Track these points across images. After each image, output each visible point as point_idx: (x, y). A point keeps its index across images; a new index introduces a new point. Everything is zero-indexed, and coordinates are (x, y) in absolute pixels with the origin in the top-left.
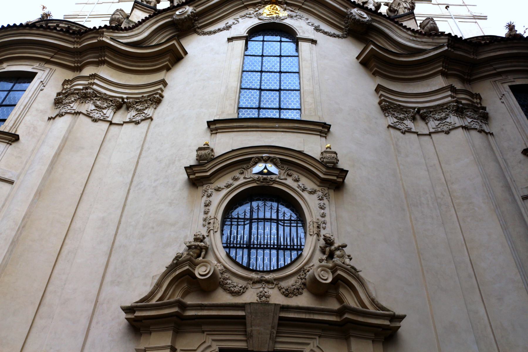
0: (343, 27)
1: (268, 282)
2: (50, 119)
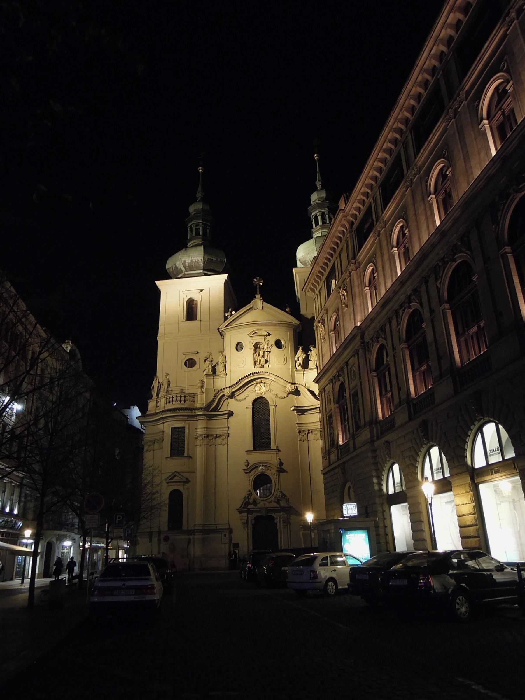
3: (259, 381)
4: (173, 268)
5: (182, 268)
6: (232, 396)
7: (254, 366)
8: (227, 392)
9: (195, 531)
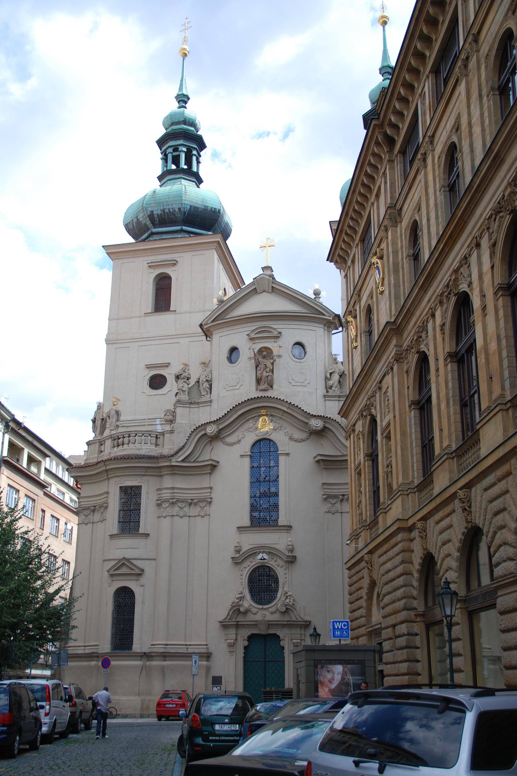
0: (307, 430)
1: (265, 609)
2: (158, 517)
3: (263, 412)
4: (134, 224)
5: (148, 223)
6: (216, 437)
7: (254, 388)
8: (211, 430)
9: (153, 654)
